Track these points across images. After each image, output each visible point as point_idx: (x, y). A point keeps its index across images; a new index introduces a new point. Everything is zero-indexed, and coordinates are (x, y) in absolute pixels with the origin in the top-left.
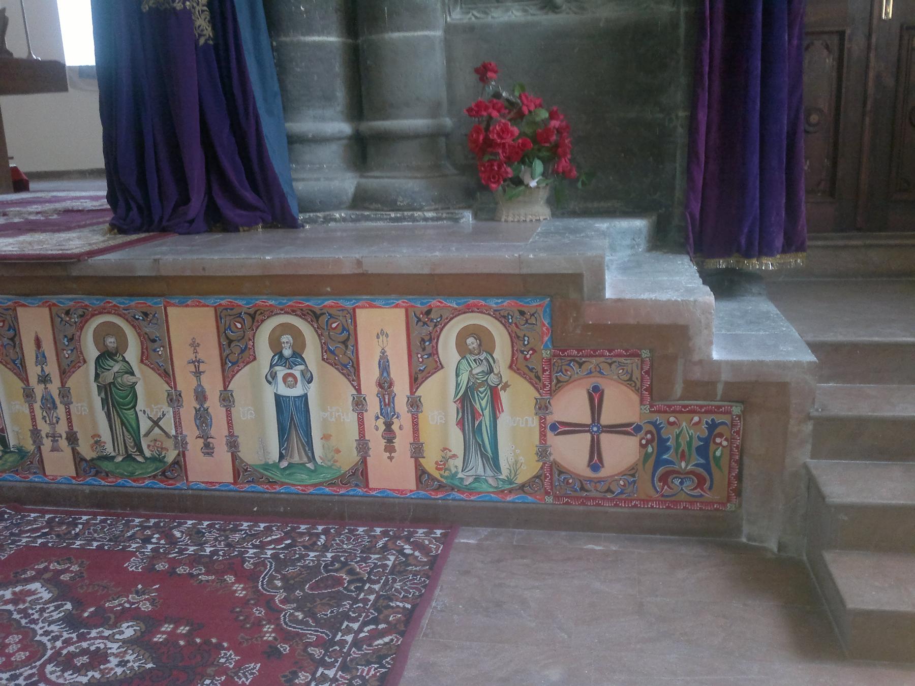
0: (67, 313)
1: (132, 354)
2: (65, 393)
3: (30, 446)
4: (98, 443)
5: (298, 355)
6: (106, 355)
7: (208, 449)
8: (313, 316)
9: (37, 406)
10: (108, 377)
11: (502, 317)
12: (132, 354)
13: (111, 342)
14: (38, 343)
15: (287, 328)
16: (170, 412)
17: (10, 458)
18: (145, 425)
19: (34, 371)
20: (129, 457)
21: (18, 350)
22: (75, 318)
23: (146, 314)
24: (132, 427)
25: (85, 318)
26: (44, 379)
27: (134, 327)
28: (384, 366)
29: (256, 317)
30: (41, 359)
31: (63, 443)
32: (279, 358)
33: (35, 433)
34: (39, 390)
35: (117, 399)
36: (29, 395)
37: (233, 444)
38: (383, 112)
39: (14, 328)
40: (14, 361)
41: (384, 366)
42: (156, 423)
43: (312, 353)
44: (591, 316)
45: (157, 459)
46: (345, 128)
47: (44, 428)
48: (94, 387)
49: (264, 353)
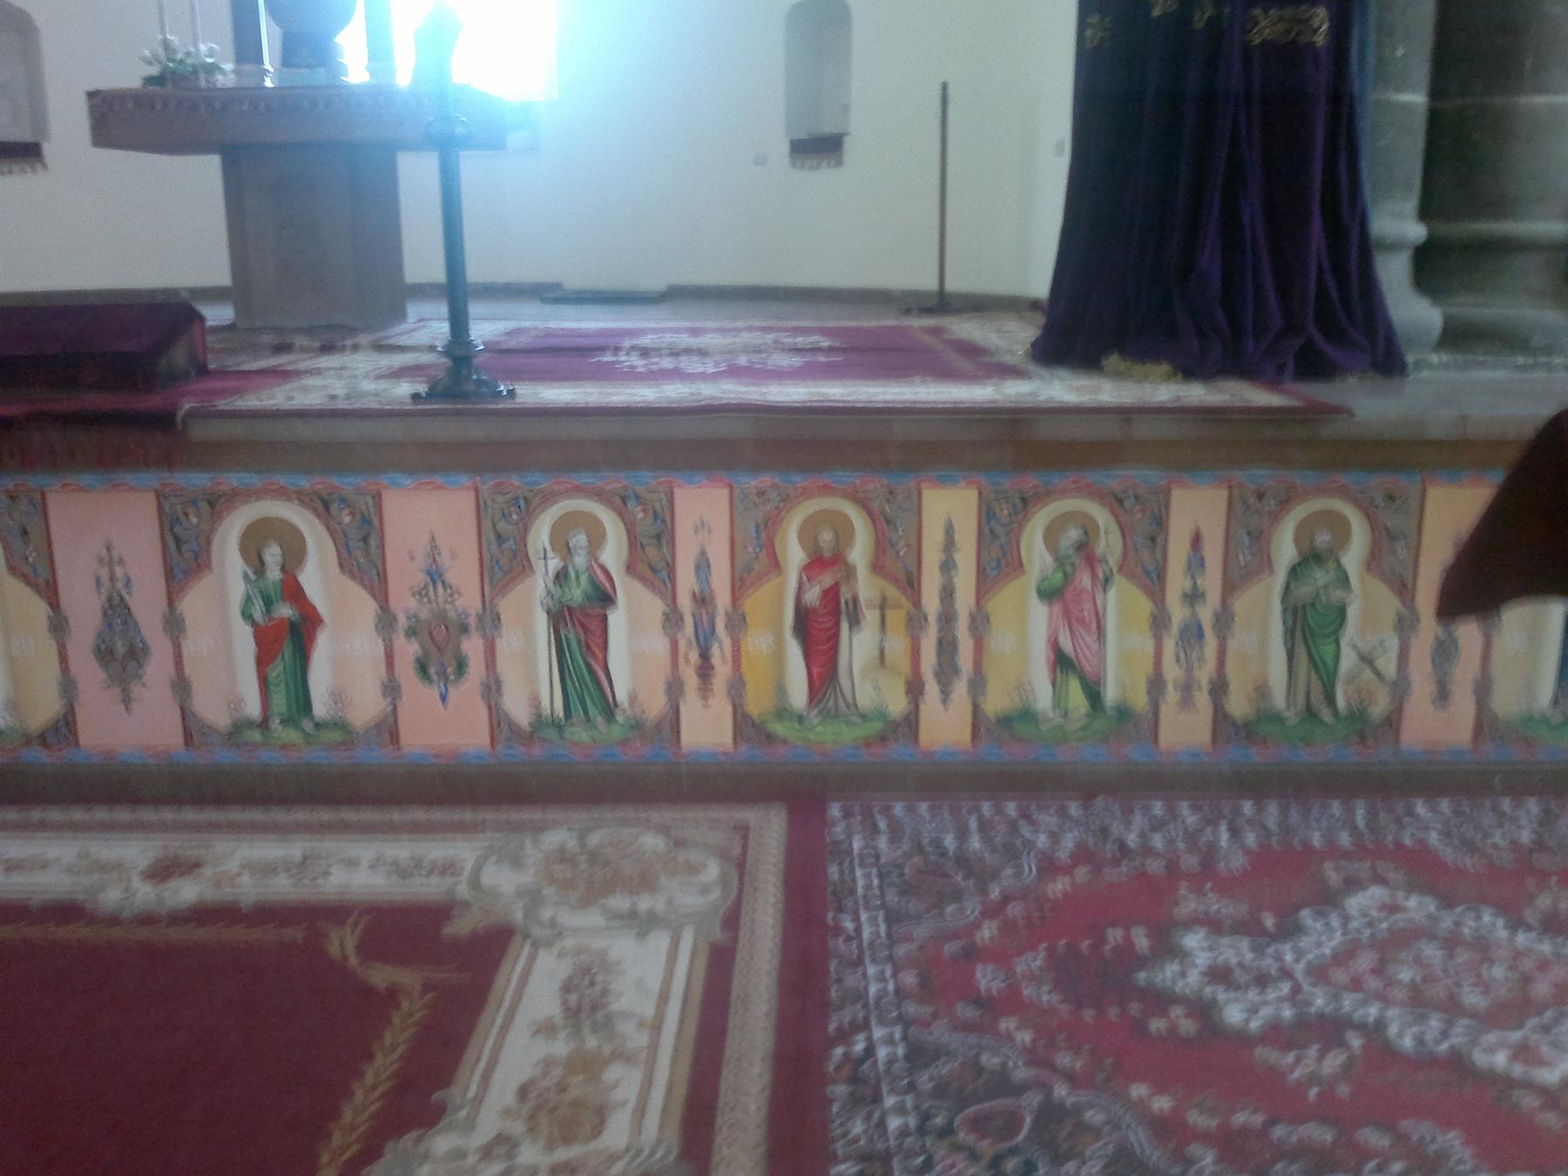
0: (1260, 496)
1: (1353, 558)
2: (1224, 620)
3: (1140, 700)
4: (1262, 691)
6: (1310, 558)
7: (1443, 695)
9: (1170, 645)
10: (1304, 591)
12: (1353, 558)
13: (1323, 539)
14: (1196, 541)
16: (1393, 643)
17: (1099, 724)
18: (1348, 660)
19: (1176, 582)
20: (1310, 713)
21: (1159, 554)
22: (1271, 503)
23: (1391, 498)
24: (1325, 667)
25: (1286, 503)
26: (1193, 597)
27: (1368, 516)
30: (1196, 563)
31: (1203, 699)
33: (1156, 684)
34: (1178, 613)
35: (1311, 625)
36: (1159, 623)
37: (1483, 688)
38: (1498, 206)
39: (1160, 522)
40: (1147, 573)
42: (1367, 660)
45: (1358, 716)
46: (1416, 232)
47: (1172, 672)
48: (1277, 607)
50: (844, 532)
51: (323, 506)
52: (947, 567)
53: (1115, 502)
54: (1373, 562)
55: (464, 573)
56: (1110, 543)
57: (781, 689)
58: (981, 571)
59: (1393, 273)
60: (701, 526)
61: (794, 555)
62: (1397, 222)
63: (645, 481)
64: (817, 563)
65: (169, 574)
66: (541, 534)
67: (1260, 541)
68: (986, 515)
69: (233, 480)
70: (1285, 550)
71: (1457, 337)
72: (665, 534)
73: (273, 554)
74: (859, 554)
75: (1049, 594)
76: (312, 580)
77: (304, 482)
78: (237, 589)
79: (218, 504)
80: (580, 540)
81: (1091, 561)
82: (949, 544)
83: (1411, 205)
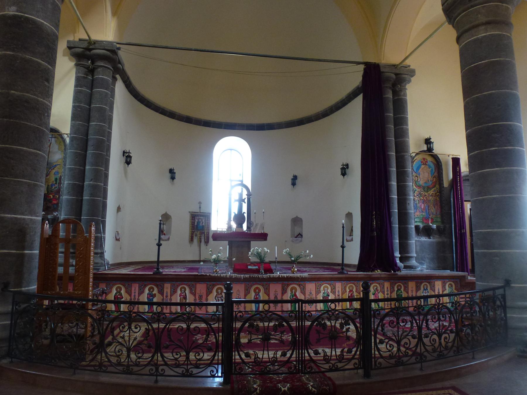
1: (402, 290)
5: (427, 289)
6: (398, 290)
8: (429, 283)
10: (398, 293)
11: (453, 282)
12: (402, 290)
15: (426, 285)
19: (386, 293)
25: (396, 284)
28: (439, 290)
29: (421, 283)
30: (387, 291)
32: (425, 289)
39: (384, 286)
41: (439, 290)
43: (429, 288)
44: (467, 281)
46: (399, 256)
49: (422, 288)
50: (353, 288)
51: (299, 285)
53: (379, 284)
54: (404, 290)
55: (314, 293)
56: (379, 288)
57: (347, 306)
59: (398, 261)
61: (348, 290)
62: (397, 254)
63: (332, 282)
64: (350, 291)
66: (322, 288)
67: (393, 288)
69: (291, 282)
70: (396, 289)
71: (406, 267)
72: (335, 288)
74: (354, 290)
75: (373, 294)
76: (297, 294)
77: (297, 282)
78: (289, 295)
80: (326, 289)
81: (377, 290)
83: (398, 253)
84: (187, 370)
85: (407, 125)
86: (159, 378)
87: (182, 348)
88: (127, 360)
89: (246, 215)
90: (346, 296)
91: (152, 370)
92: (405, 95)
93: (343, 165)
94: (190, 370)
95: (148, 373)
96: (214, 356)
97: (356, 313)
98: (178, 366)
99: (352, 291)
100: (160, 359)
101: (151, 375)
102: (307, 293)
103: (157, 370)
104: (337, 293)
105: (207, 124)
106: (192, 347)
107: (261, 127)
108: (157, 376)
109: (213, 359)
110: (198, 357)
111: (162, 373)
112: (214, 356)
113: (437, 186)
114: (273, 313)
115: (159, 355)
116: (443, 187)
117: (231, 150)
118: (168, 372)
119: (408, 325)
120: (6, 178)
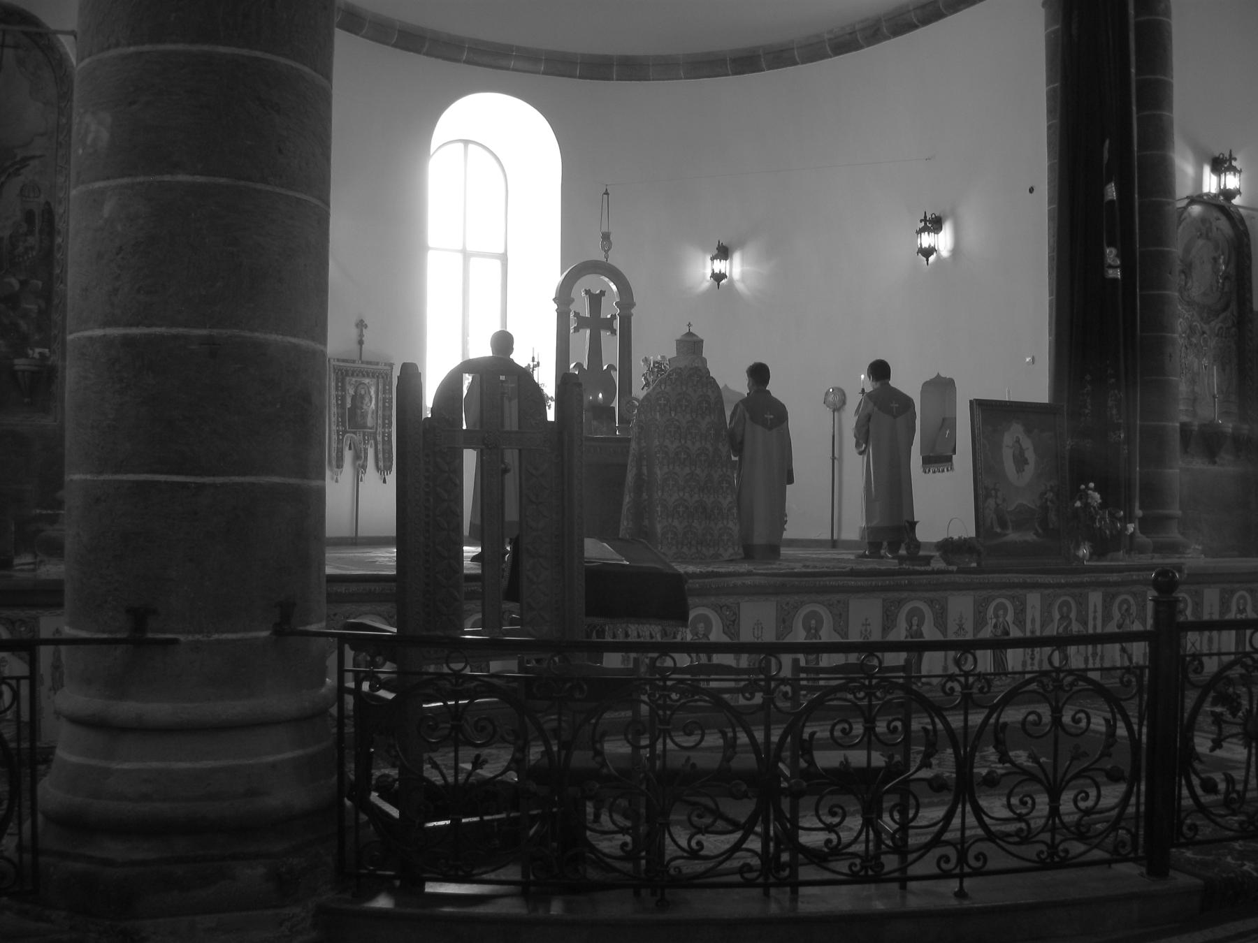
29: (1233, 592)
52: (1095, 618)
55: (969, 626)
58: (1103, 621)
60: (1033, 607)
61: (1057, 616)
64: (1062, 617)
65: (884, 629)
68: (1104, 601)
69: (905, 595)
72: (1023, 611)
73: (915, 621)
74: (1073, 615)
77: (927, 595)
79: (900, 603)
80: (1001, 612)
82: (1095, 612)
84: (1053, 847)
85: (1171, 110)
86: (967, 882)
87: (1040, 781)
88: (863, 837)
89: (616, 375)
90: (1052, 630)
91: (948, 860)
92: (1167, 12)
93: (925, 220)
94: (1061, 847)
95: (936, 871)
96: (948, 818)
97: (1129, 681)
98: (1025, 838)
99: (1068, 616)
100: (971, 820)
101: (946, 875)
102: (952, 627)
103: (962, 859)
104: (1029, 626)
105: (410, 39)
106: (1068, 777)
107: (598, 68)
108: (961, 876)
109: (944, 830)
110: (1082, 805)
111: (978, 864)
112: (948, 818)
113: (1233, 306)
114: (1081, 675)
115: (968, 808)
116: (1251, 309)
117: (466, 142)
118: (997, 860)
119: (1098, 724)
120: (259, 186)
